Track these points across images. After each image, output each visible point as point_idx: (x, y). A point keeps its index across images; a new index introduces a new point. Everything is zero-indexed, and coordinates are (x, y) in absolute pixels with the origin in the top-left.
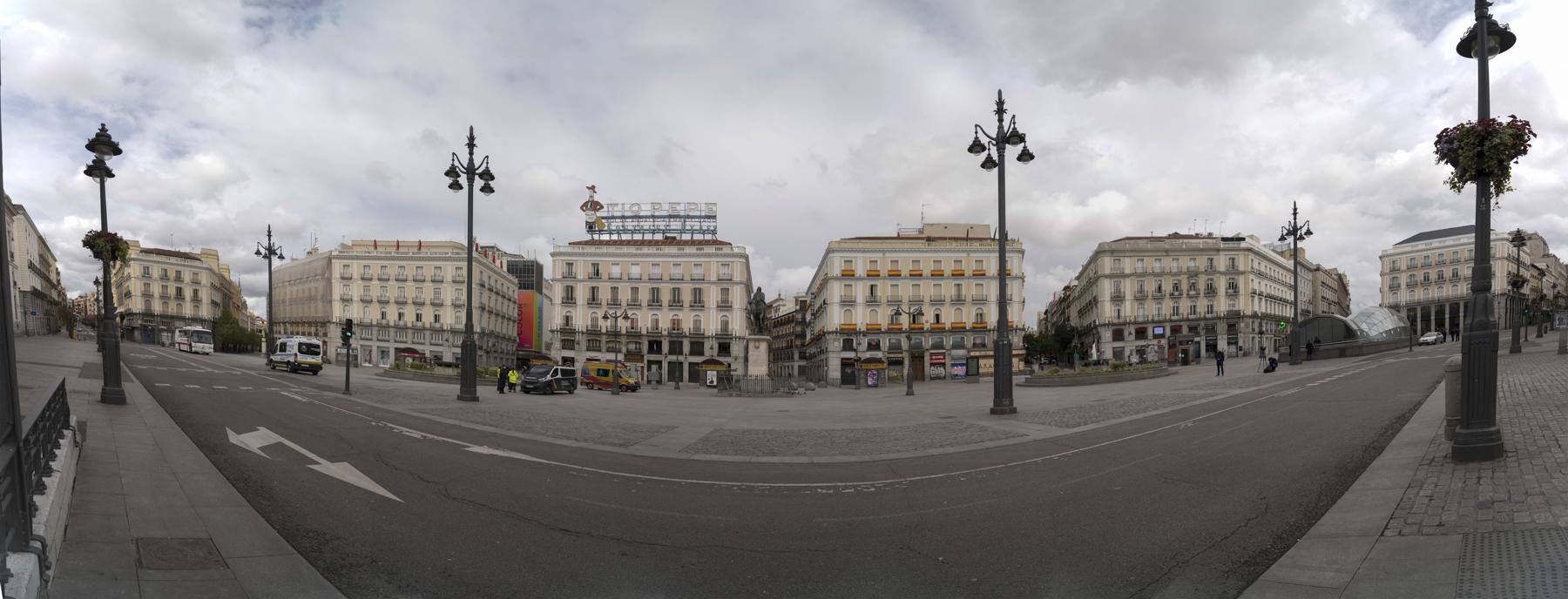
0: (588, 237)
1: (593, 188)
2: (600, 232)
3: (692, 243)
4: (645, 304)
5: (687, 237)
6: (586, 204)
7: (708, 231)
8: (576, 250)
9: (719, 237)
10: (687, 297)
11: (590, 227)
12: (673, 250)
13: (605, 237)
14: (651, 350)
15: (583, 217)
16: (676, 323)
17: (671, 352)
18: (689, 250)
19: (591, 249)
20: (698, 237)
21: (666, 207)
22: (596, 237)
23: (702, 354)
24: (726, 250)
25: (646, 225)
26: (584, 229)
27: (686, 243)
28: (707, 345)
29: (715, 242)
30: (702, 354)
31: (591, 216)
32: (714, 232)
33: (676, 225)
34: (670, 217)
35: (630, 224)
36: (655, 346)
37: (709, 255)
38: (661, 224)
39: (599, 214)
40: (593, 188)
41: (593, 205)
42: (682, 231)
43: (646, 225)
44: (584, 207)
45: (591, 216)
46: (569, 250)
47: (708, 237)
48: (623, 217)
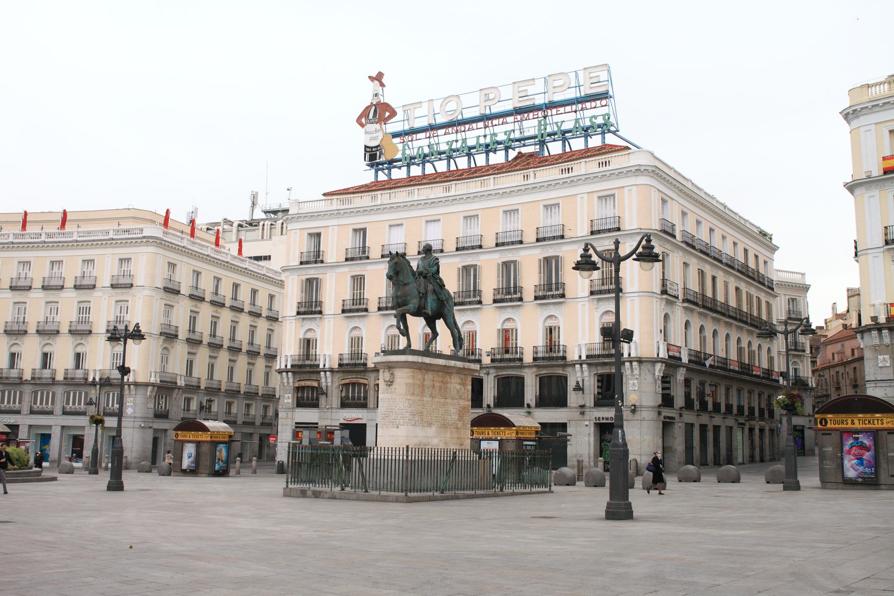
0: (368, 176)
1: (378, 78)
4: (373, 306)
6: (365, 113)
8: (336, 204)
10: (530, 279)
11: (372, 155)
13: (398, 174)
15: (362, 137)
17: (543, 402)
19: (383, 198)
24: (617, 161)
25: (473, 136)
26: (361, 163)
31: (374, 135)
34: (518, 111)
35: (443, 140)
36: (510, 391)
38: (501, 130)
40: (378, 78)
41: (379, 112)
43: (473, 136)
44: (364, 118)
45: (374, 135)
46: (323, 206)
48: (433, 128)
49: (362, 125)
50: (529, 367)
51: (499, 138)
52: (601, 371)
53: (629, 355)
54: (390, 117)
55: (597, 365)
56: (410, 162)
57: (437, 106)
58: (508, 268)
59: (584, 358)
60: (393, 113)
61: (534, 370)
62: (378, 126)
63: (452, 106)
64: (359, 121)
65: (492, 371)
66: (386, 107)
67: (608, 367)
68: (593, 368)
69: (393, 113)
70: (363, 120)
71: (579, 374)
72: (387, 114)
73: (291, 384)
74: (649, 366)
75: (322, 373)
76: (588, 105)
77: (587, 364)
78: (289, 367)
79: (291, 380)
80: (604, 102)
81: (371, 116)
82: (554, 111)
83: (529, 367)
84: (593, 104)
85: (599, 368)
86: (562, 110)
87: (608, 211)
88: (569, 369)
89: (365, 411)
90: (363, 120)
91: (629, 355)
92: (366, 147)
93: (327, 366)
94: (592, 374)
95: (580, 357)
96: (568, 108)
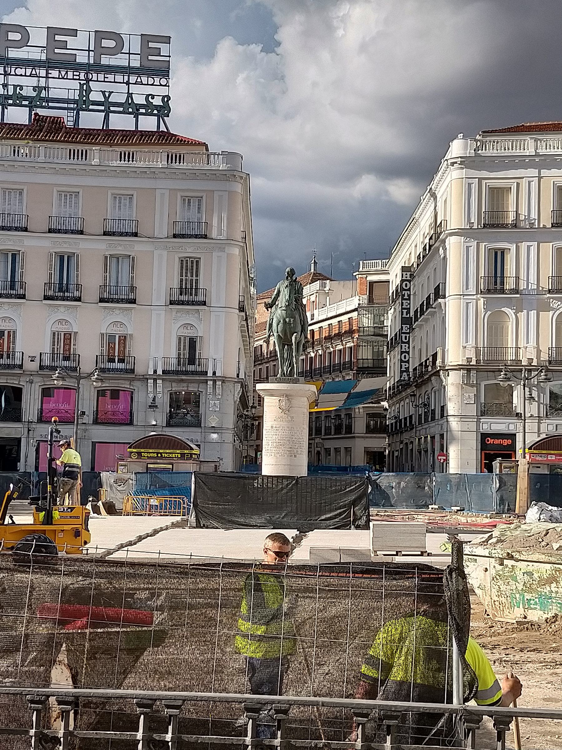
3: (107, 136)
5: (91, 120)
7: (149, 108)
9: (175, 125)
10: (90, 278)
12: (59, 152)
18: (96, 155)
20: (121, 122)
21: (39, 38)
23: (128, 421)
27: (90, 136)
28: (142, 396)
29: (164, 138)
30: (128, 421)
32: (163, 111)
33: (64, 87)
37: (151, 173)
38: (27, 83)
42: (82, 104)
47: (148, 123)
51: (24, 93)
52: (176, 387)
53: (214, 373)
55: (172, 381)
58: (64, 261)
59: (160, 372)
65: (36, 379)
67: (185, 385)
68: (168, 384)
71: (150, 389)
74: (231, 385)
76: (144, 79)
77: (163, 380)
80: (163, 82)
82: (101, 77)
84: (151, 81)
85: (174, 384)
86: (111, 77)
87: (193, 214)
88: (137, 384)
91: (214, 373)
94: (166, 391)
95: (155, 372)
96: (119, 78)
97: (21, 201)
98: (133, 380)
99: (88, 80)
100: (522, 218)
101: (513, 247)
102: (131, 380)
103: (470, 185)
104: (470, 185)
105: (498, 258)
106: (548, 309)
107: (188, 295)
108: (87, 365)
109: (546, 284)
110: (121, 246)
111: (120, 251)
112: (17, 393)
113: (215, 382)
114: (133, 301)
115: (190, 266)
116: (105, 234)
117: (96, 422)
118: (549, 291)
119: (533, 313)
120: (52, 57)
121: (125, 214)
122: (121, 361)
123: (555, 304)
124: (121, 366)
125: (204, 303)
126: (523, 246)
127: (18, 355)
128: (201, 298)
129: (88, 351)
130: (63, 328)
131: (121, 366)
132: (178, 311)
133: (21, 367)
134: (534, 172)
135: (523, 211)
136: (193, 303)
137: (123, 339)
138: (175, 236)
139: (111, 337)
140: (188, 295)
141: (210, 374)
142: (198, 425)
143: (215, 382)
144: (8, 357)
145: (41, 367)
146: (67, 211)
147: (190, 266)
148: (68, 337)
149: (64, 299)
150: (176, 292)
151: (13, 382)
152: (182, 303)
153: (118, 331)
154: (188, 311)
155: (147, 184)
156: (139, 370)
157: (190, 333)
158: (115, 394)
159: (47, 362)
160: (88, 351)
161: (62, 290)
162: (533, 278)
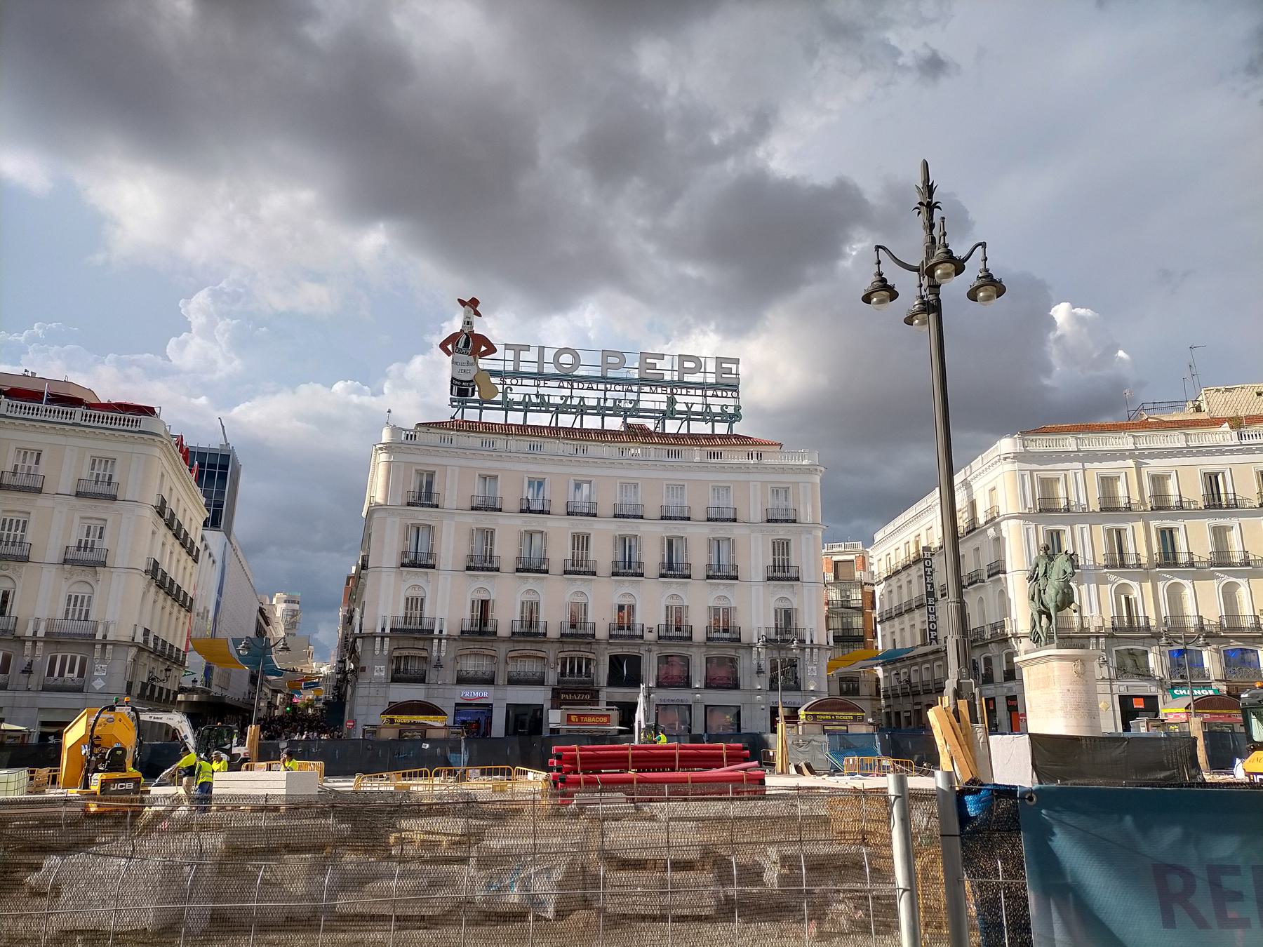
2: (482, 405)
6: (453, 338)
10: (698, 558)
11: (461, 390)
13: (494, 417)
14: (615, 679)
16: (677, 617)
22: (471, 415)
39: (484, 364)
49: (448, 353)
50: (699, 646)
54: (485, 353)
56: (507, 406)
57: (549, 356)
60: (492, 349)
61: (704, 649)
62: (471, 359)
63: (566, 359)
64: (443, 346)
66: (482, 340)
69: (492, 349)
70: (450, 347)
72: (483, 348)
73: (386, 653)
75: (436, 641)
78: (388, 630)
79: (386, 647)
81: (461, 345)
83: (699, 646)
88: (742, 651)
89: (491, 688)
90: (450, 347)
92: (453, 379)
93: (445, 632)
97: (635, 493)
98: (739, 647)
99: (673, 394)
100: (1073, 503)
101: (1068, 529)
102: (736, 648)
103: (1023, 476)
104: (1023, 476)
105: (1055, 536)
106: (1106, 582)
107: (782, 573)
108: (699, 636)
109: (1101, 561)
110: (722, 530)
111: (721, 534)
112: (635, 662)
113: (812, 649)
114: (736, 578)
115: (781, 547)
116: (709, 520)
117: (708, 686)
118: (1106, 567)
119: (1093, 586)
120: (644, 376)
121: (723, 503)
122: (725, 631)
123: (1112, 578)
124: (726, 635)
125: (797, 579)
126: (1077, 527)
127: (638, 627)
128: (795, 575)
129: (699, 623)
130: (676, 602)
131: (726, 635)
132: (775, 586)
133: (642, 637)
134: (1079, 465)
135: (1073, 498)
136: (788, 579)
137: (727, 611)
138: (768, 521)
139: (716, 610)
140: (782, 573)
141: (808, 642)
142: (798, 688)
143: (812, 649)
144: (629, 628)
145: (660, 638)
146: (673, 501)
147: (781, 547)
148: (680, 610)
149: (675, 576)
150: (771, 569)
151: (633, 651)
152: (779, 579)
153: (722, 604)
154: (783, 586)
155: (742, 477)
156: (744, 639)
157: (786, 606)
158: (722, 660)
159: (662, 634)
160: (699, 623)
161: (672, 569)
162: (1089, 555)
